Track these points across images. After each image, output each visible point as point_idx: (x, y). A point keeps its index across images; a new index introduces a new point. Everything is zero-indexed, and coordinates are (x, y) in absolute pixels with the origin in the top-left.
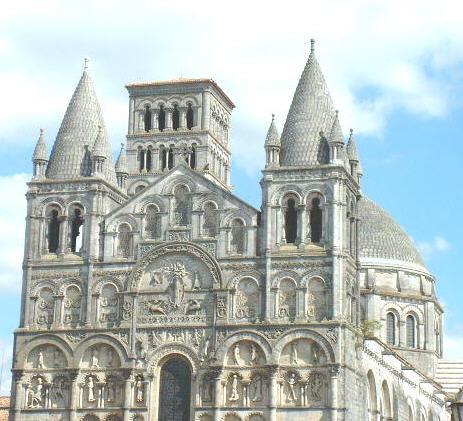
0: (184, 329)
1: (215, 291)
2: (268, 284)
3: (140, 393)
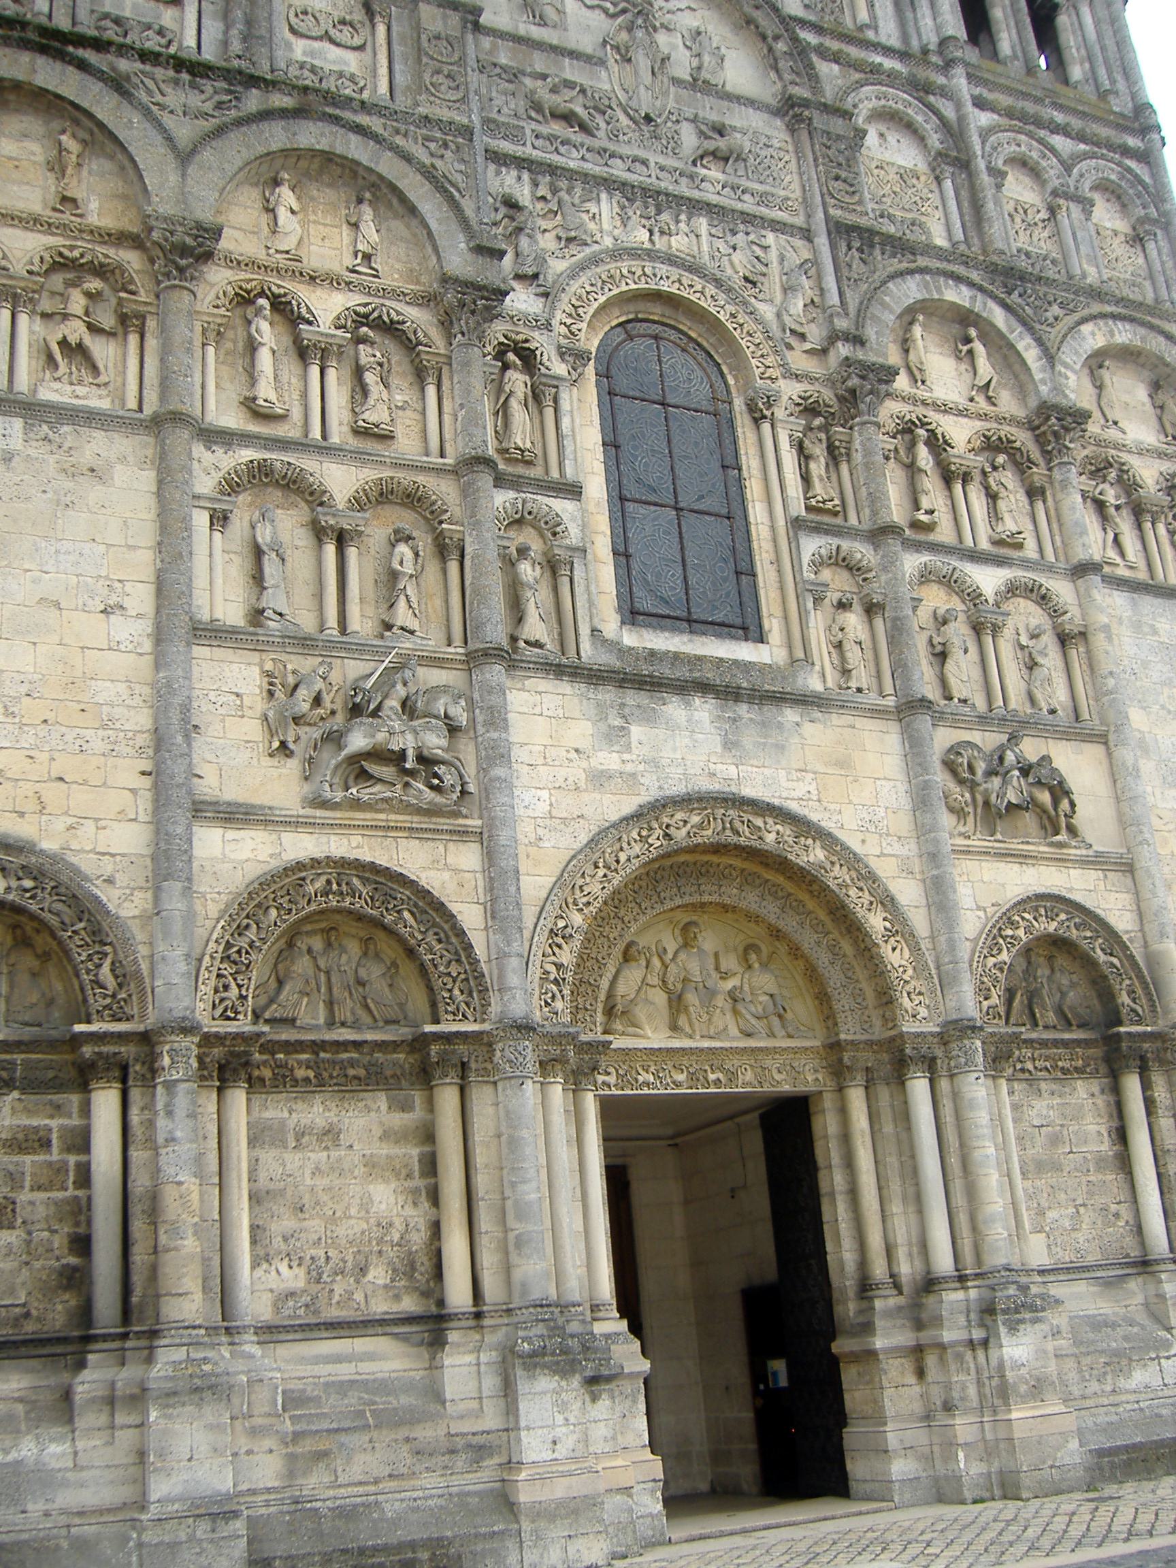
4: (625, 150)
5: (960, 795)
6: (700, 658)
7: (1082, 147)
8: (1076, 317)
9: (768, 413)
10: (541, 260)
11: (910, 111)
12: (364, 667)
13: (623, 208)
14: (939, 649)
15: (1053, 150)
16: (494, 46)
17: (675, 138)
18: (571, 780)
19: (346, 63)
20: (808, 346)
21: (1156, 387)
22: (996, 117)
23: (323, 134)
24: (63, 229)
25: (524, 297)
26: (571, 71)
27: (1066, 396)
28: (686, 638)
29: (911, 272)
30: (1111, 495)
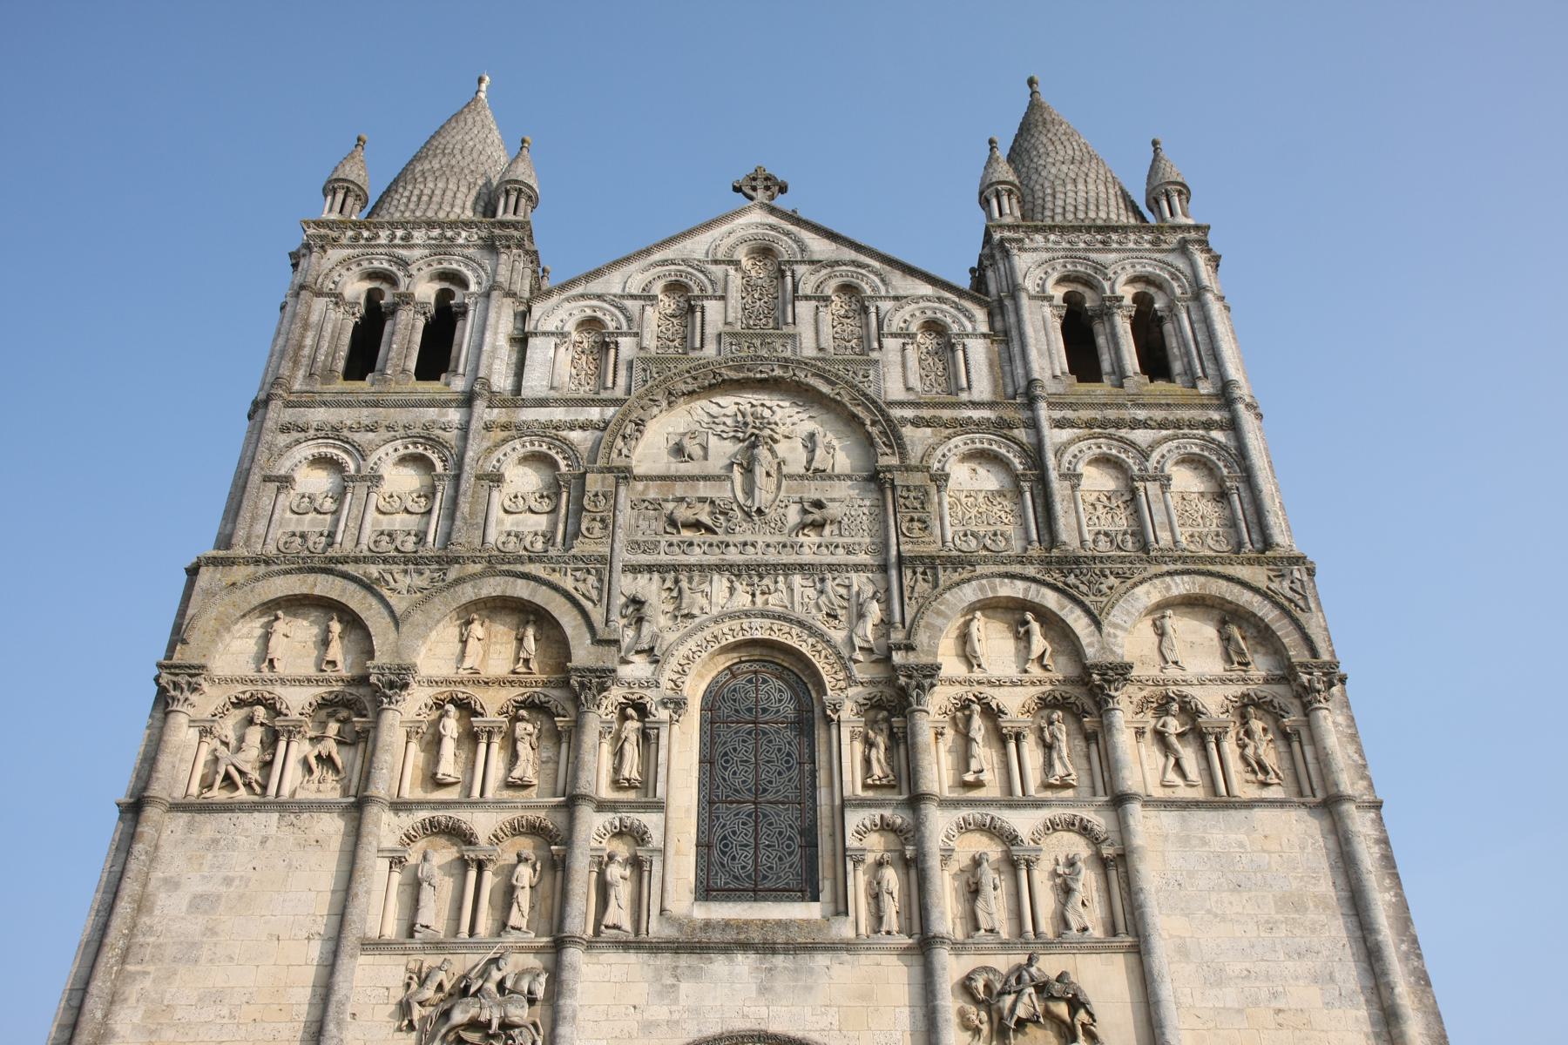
0: (788, 569)
1: (889, 469)
2: (1051, 461)
3: (631, 752)
4: (739, 538)
5: (978, 1016)
6: (747, 923)
7: (1164, 432)
8: (1129, 583)
9: (835, 717)
10: (655, 637)
11: (995, 447)
12: (476, 958)
13: (732, 582)
14: (973, 887)
15: (1132, 444)
16: (646, 487)
17: (783, 518)
18: (625, 1031)
19: (540, 525)
20: (874, 657)
21: (1222, 624)
22: (1075, 430)
23: (499, 585)
24: (328, 681)
25: (641, 666)
26: (704, 489)
27: (1113, 652)
28: (746, 905)
29: (969, 580)
30: (1174, 726)
